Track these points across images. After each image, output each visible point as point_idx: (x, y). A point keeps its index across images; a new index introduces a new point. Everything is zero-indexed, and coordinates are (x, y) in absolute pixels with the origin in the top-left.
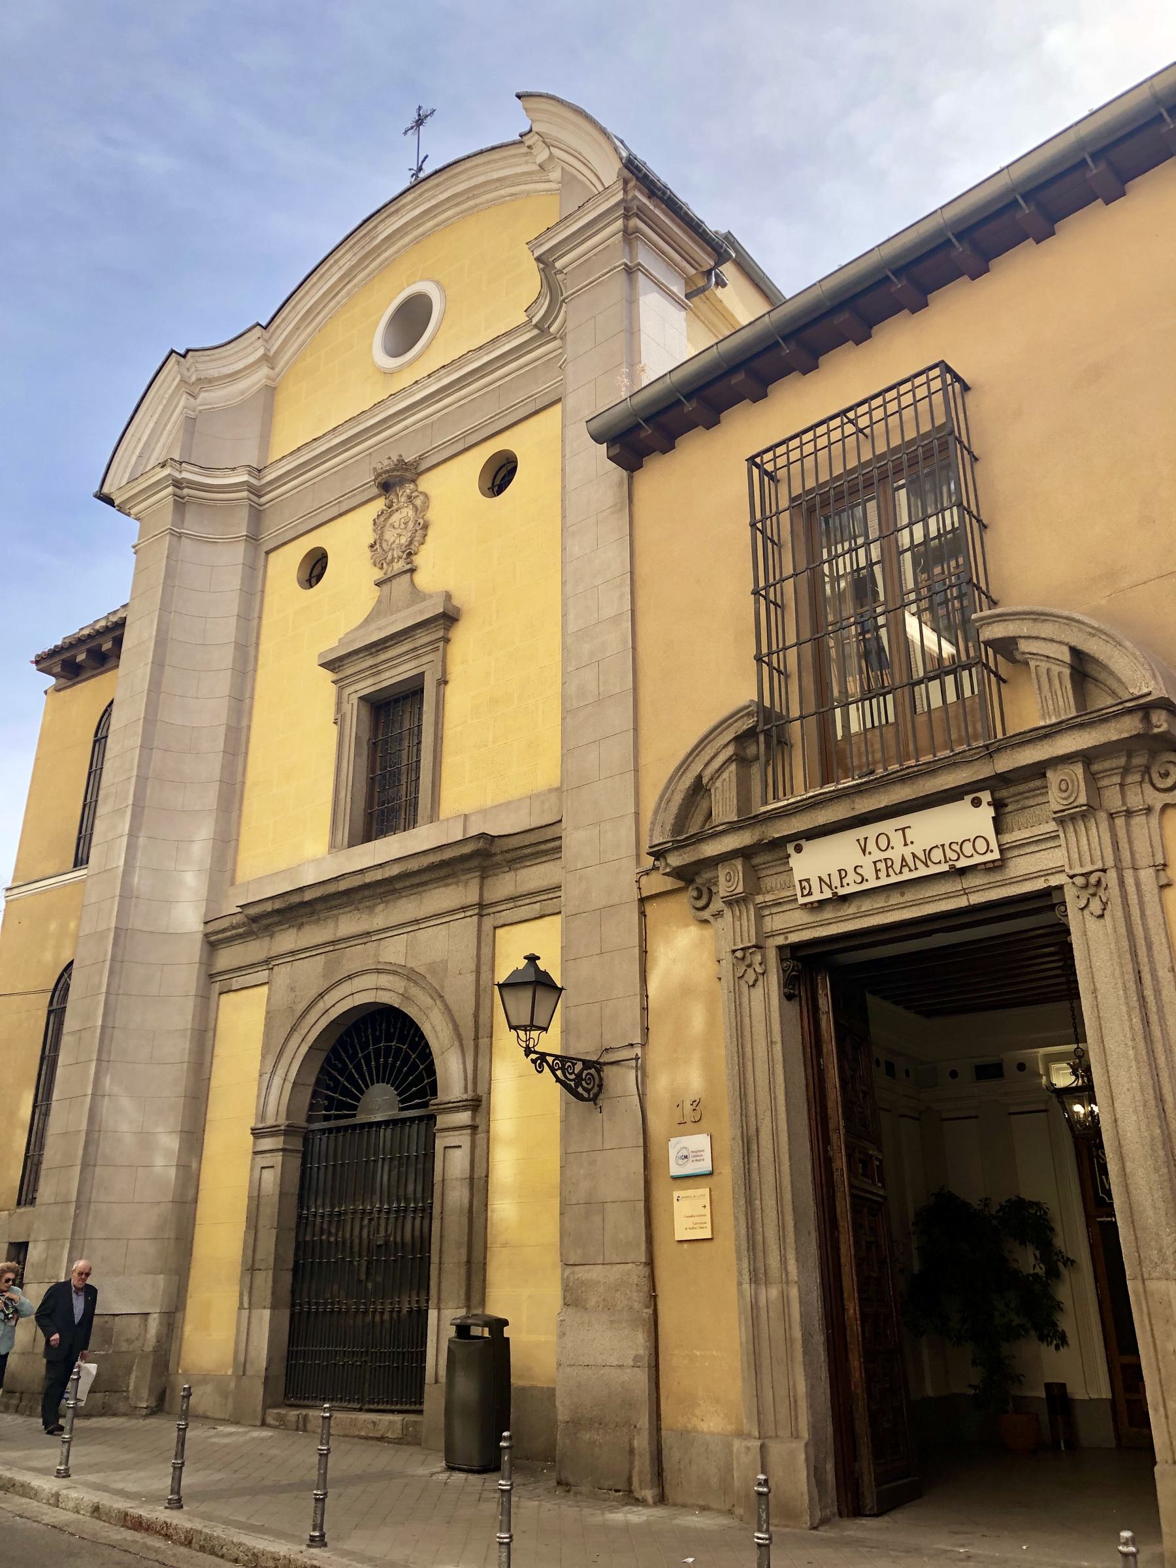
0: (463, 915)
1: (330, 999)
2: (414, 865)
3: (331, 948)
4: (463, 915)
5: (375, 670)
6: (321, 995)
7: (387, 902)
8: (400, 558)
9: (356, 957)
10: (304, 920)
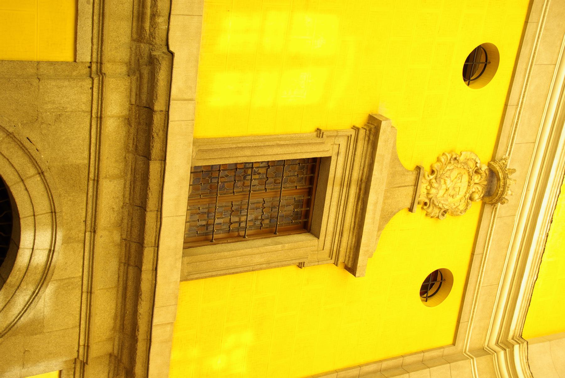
0: (82, 343)
1: (35, 185)
2: (143, 308)
3: (92, 176)
4: (82, 343)
5: (346, 184)
6: (41, 173)
7: (120, 245)
8: (428, 194)
9: (73, 208)
10: (133, 131)
